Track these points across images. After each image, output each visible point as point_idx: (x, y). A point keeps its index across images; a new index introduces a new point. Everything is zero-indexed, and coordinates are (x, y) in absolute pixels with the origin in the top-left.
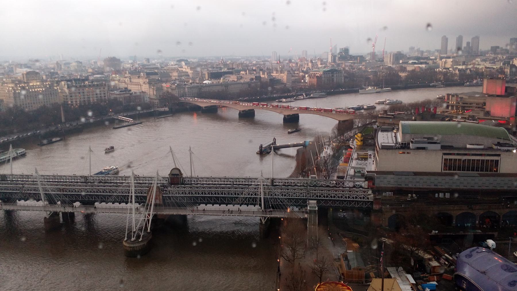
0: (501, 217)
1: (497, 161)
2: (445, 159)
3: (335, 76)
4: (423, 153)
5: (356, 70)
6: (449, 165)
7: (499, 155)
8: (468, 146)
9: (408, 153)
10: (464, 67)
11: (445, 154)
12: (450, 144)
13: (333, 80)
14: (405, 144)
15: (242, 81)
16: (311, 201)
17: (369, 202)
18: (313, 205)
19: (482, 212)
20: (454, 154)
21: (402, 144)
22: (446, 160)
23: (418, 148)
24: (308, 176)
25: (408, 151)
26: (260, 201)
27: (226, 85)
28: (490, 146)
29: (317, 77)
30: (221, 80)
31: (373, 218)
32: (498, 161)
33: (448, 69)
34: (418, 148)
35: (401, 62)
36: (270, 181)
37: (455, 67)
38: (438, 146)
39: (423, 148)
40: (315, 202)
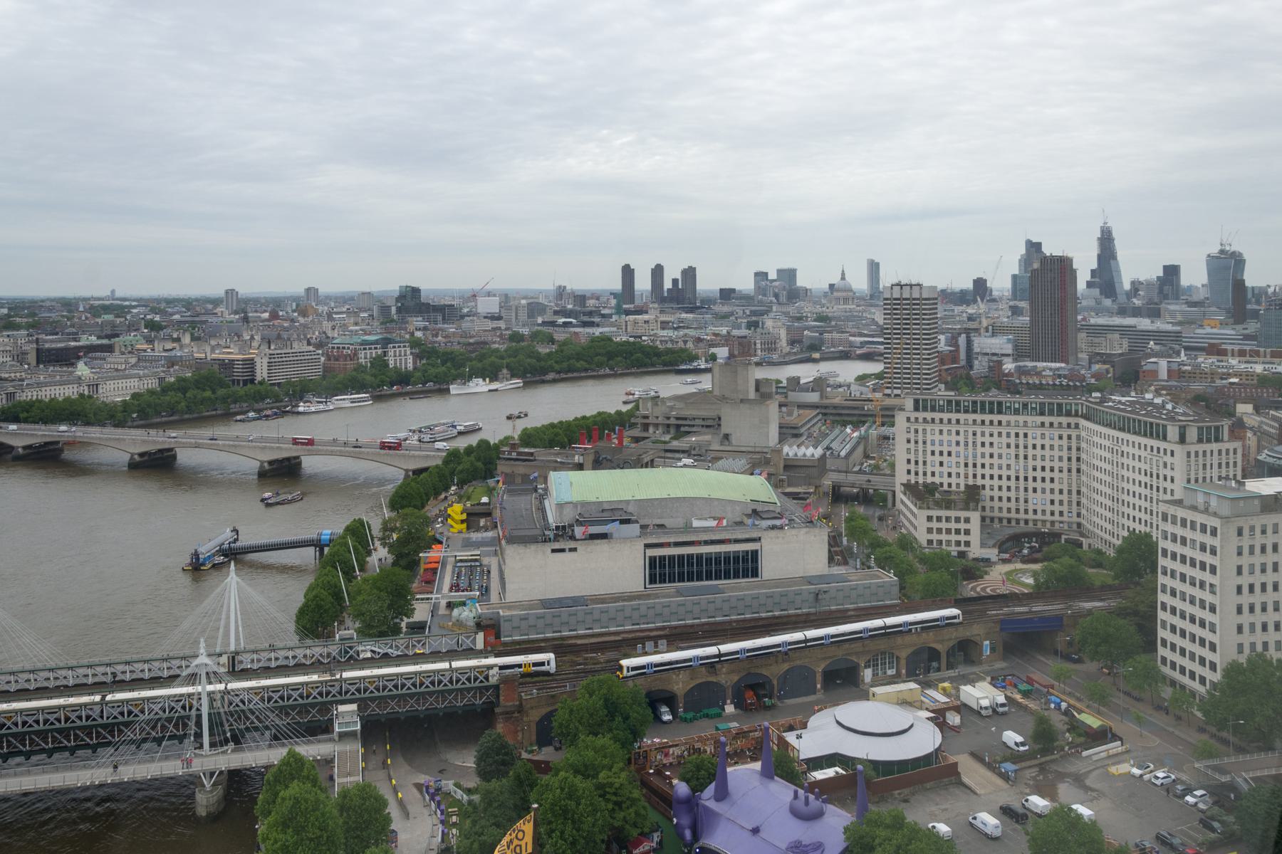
0: (775, 682)
2: (650, 558)
4: (601, 546)
6: (660, 571)
8: (696, 523)
9: (571, 550)
11: (647, 546)
12: (659, 522)
14: (564, 527)
16: (342, 708)
17: (487, 688)
18: (347, 719)
19: (736, 678)
20: (668, 545)
21: (557, 528)
22: (653, 560)
23: (593, 537)
24: (330, 636)
25: (572, 544)
26: (199, 724)
28: (738, 520)
31: (500, 728)
32: (757, 551)
34: (593, 537)
36: (224, 659)
38: (634, 529)
39: (604, 536)
40: (354, 707)
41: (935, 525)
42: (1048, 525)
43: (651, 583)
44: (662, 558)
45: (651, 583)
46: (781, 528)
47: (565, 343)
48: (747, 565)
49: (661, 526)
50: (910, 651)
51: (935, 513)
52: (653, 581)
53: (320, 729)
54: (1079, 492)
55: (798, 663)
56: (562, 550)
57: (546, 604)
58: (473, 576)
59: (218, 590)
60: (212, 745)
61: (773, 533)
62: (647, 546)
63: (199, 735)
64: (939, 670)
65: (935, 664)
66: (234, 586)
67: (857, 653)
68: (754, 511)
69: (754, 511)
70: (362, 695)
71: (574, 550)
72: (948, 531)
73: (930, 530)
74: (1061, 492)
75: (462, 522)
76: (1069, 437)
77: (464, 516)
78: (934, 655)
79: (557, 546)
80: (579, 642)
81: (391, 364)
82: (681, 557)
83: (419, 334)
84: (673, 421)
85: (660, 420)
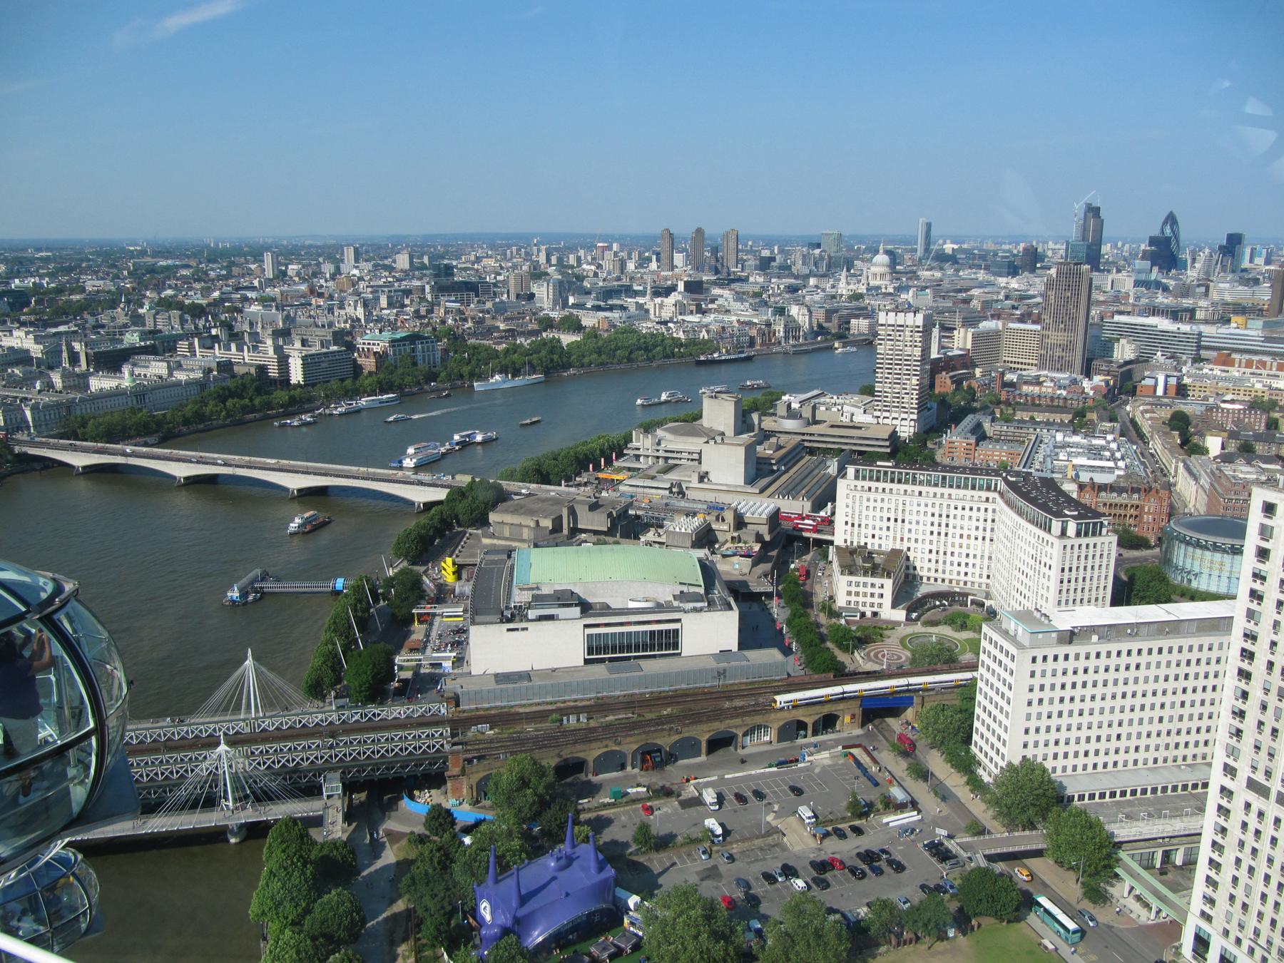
1: (676, 632)
5: (470, 324)
7: (679, 620)
8: (632, 605)
9: (523, 629)
10: (695, 318)
11: (586, 626)
15: (181, 376)
19: (635, 747)
25: (524, 625)
27: (140, 393)
29: (375, 353)
30: (125, 379)
33: (665, 323)
34: (541, 618)
35: (571, 300)
37: (680, 318)
41: (853, 589)
42: (962, 584)
46: (701, 610)
47: (593, 334)
48: (670, 641)
50: (782, 723)
51: (854, 579)
52: (590, 651)
53: (313, 791)
54: (990, 558)
55: (687, 735)
57: (501, 678)
60: (235, 800)
61: (692, 615)
62: (586, 626)
63: (226, 791)
64: (805, 736)
65: (802, 732)
67: (737, 727)
68: (682, 592)
69: (682, 592)
70: (344, 768)
72: (865, 595)
73: (849, 593)
74: (975, 556)
76: (986, 510)
78: (801, 725)
79: (511, 626)
80: (521, 710)
84: (661, 454)
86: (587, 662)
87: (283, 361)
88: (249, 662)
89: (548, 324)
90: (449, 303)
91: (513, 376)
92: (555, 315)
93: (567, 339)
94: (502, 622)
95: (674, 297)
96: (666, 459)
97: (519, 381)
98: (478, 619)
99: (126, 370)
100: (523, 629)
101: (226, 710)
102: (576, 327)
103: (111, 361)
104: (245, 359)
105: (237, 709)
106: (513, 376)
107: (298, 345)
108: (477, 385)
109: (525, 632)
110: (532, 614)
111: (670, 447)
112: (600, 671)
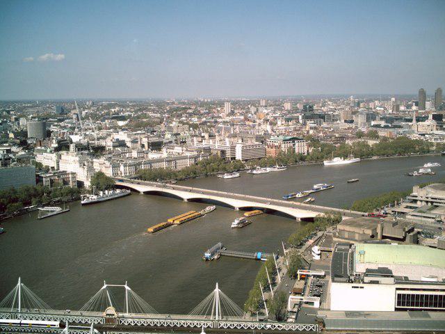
3: (297, 145)
6: (404, 301)
9: (361, 287)
13: (294, 151)
14: (359, 275)
22: (399, 295)
30: (164, 153)
34: (372, 282)
39: (377, 282)
43: (398, 305)
44: (404, 295)
45: (398, 305)
47: (385, 139)
49: (406, 278)
52: (399, 304)
56: (358, 287)
57: (348, 314)
58: (320, 291)
59: (212, 294)
62: (397, 289)
66: (217, 294)
71: (363, 287)
75: (318, 255)
77: (319, 252)
81: (296, 151)
82: (413, 295)
83: (311, 132)
85: (424, 199)
86: (396, 309)
87: (233, 148)
88: (217, 290)
89: (360, 135)
90: (310, 124)
91: (344, 159)
92: (364, 130)
93: (371, 143)
94: (349, 282)
95: (427, 123)
96: (432, 203)
97: (347, 162)
98: (336, 279)
99: (164, 150)
100: (361, 287)
101: (203, 314)
102: (374, 135)
103: (156, 146)
104: (216, 145)
105: (209, 314)
106: (344, 159)
107: (240, 141)
108: (326, 163)
109: (362, 289)
110: (367, 279)
111: (434, 196)
112: (405, 316)
